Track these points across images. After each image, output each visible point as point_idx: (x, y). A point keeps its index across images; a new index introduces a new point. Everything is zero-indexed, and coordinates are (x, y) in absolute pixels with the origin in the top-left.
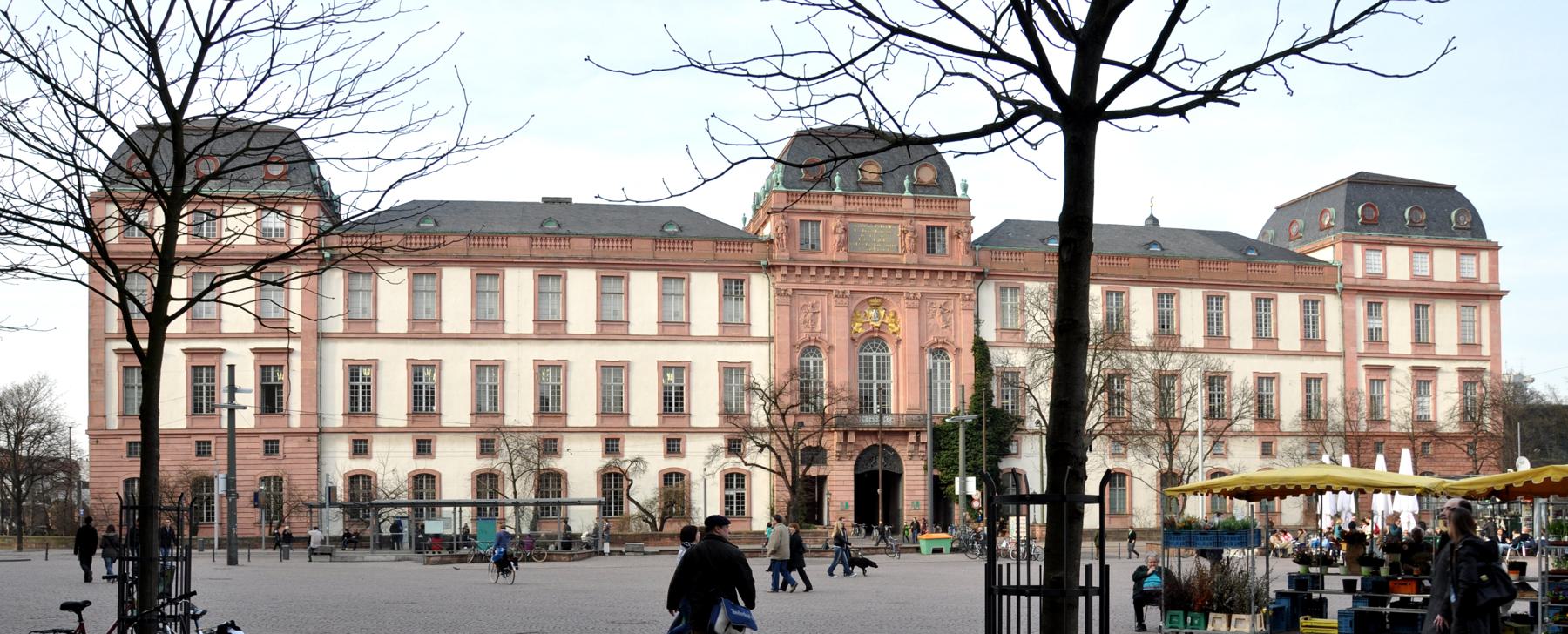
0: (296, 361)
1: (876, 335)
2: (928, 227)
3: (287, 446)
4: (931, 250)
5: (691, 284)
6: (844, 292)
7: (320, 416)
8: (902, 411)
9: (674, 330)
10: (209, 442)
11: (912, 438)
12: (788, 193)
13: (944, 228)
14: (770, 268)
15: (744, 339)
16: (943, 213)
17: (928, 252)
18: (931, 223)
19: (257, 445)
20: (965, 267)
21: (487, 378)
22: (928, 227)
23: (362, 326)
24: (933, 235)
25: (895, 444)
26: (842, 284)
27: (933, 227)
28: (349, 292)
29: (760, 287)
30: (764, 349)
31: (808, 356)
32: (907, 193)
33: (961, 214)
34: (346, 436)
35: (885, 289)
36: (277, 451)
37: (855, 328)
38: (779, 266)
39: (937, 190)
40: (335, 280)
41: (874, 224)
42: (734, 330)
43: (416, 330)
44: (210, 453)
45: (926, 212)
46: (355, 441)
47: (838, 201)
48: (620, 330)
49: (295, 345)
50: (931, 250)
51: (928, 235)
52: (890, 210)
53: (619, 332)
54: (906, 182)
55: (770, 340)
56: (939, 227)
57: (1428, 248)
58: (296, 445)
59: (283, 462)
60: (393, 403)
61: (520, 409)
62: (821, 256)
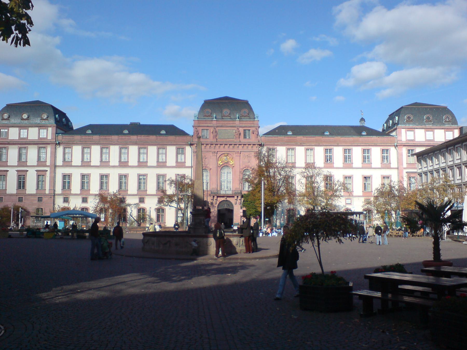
0: (48, 173)
2: (244, 130)
3: (44, 199)
4: (245, 137)
5: (167, 150)
6: (215, 152)
7: (54, 191)
8: (234, 190)
9: (162, 164)
10: (22, 198)
11: (236, 197)
12: (198, 120)
13: (249, 130)
14: (191, 145)
15: (184, 167)
16: (250, 125)
17: (244, 138)
18: (245, 128)
19: (36, 199)
20: (256, 142)
21: (104, 178)
22: (244, 130)
23: (67, 163)
24: (246, 132)
25: (232, 200)
26: (214, 149)
27: (246, 130)
28: (64, 154)
29: (188, 150)
30: (189, 170)
33: (255, 126)
34: (62, 196)
36: (42, 201)
37: (219, 163)
38: (194, 144)
39: (248, 118)
40: (60, 150)
41: (226, 130)
42: (180, 165)
43: (83, 165)
44: (22, 201)
45: (244, 125)
46: (64, 198)
47: (214, 123)
48: (144, 164)
49: (48, 169)
50: (245, 137)
51: (244, 132)
52: (231, 125)
53: (144, 165)
54: (237, 116)
55: (192, 167)
56: (248, 130)
57: (432, 129)
58: (47, 199)
59: (43, 204)
60: (76, 187)
61: (113, 188)
62: (209, 140)
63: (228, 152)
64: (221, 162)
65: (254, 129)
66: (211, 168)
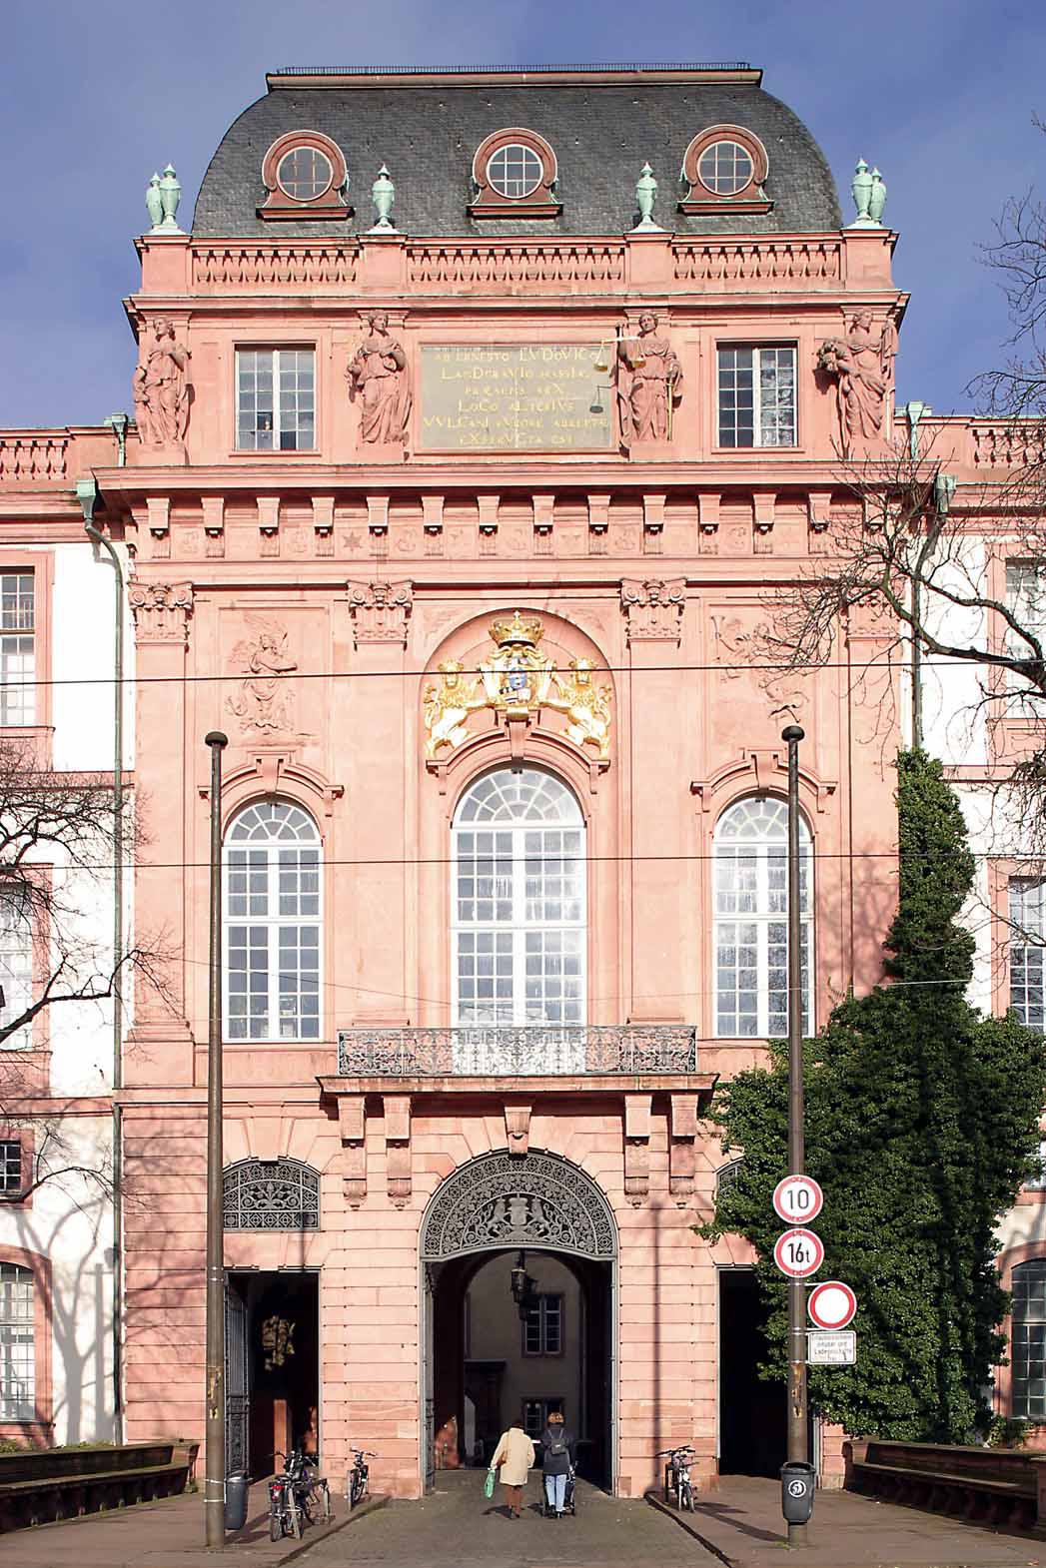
1: (518, 749)
27: (746, 346)
31: (260, 834)
32: (647, 226)
35: (547, 573)
38: (140, 498)
45: (716, 291)
63: (536, 600)
64: (461, 714)
65: (831, 328)
66: (337, 780)
